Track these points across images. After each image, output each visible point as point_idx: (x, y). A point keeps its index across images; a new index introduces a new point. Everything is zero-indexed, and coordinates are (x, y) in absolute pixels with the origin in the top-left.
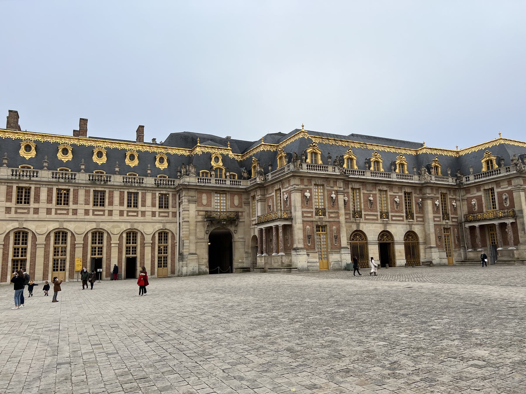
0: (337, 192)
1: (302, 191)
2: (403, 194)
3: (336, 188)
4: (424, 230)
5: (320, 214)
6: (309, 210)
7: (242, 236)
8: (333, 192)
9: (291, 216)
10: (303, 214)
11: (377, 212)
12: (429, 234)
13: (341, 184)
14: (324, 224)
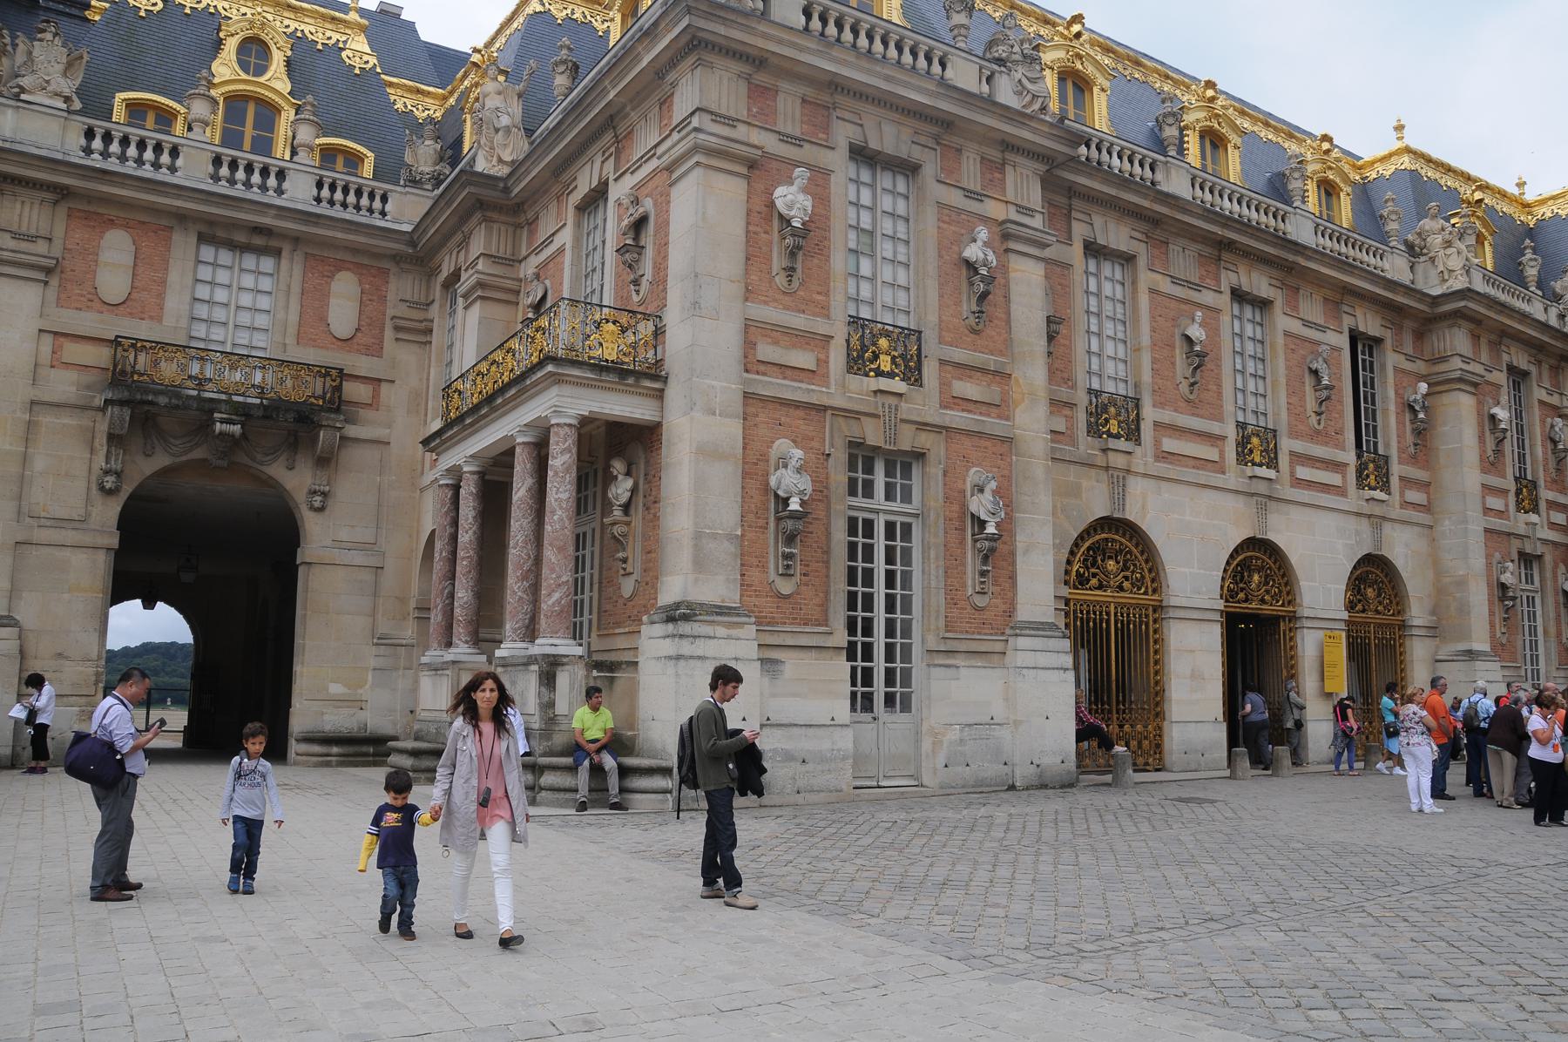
0: (1006, 236)
1: (755, 167)
2: (1344, 342)
3: (995, 210)
4: (1436, 563)
5: (885, 363)
6: (798, 321)
7: (365, 534)
8: (983, 234)
9: (659, 363)
10: (749, 345)
11: (1219, 418)
12: (1462, 583)
13: (1024, 187)
14: (907, 440)
